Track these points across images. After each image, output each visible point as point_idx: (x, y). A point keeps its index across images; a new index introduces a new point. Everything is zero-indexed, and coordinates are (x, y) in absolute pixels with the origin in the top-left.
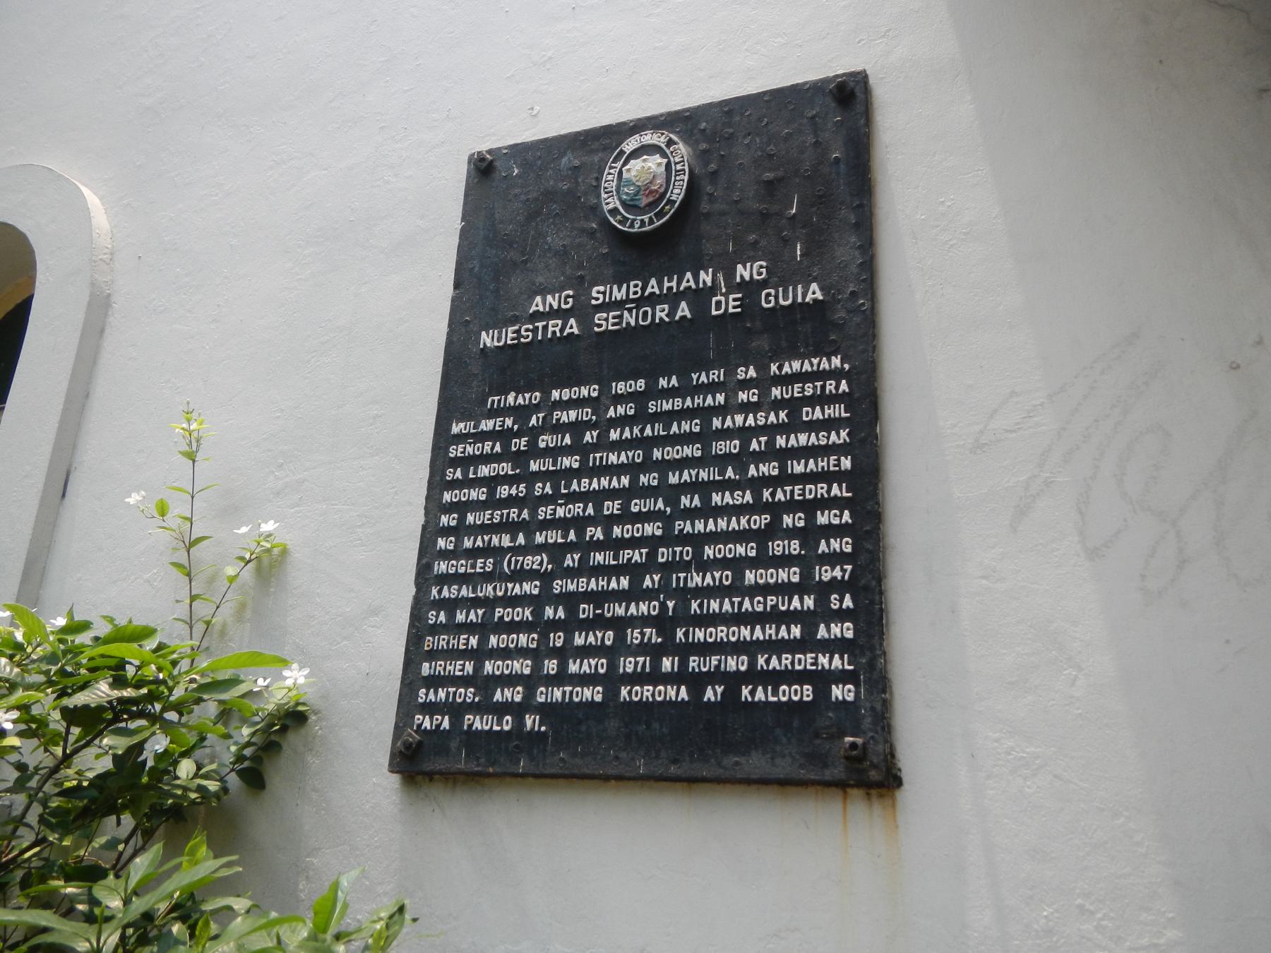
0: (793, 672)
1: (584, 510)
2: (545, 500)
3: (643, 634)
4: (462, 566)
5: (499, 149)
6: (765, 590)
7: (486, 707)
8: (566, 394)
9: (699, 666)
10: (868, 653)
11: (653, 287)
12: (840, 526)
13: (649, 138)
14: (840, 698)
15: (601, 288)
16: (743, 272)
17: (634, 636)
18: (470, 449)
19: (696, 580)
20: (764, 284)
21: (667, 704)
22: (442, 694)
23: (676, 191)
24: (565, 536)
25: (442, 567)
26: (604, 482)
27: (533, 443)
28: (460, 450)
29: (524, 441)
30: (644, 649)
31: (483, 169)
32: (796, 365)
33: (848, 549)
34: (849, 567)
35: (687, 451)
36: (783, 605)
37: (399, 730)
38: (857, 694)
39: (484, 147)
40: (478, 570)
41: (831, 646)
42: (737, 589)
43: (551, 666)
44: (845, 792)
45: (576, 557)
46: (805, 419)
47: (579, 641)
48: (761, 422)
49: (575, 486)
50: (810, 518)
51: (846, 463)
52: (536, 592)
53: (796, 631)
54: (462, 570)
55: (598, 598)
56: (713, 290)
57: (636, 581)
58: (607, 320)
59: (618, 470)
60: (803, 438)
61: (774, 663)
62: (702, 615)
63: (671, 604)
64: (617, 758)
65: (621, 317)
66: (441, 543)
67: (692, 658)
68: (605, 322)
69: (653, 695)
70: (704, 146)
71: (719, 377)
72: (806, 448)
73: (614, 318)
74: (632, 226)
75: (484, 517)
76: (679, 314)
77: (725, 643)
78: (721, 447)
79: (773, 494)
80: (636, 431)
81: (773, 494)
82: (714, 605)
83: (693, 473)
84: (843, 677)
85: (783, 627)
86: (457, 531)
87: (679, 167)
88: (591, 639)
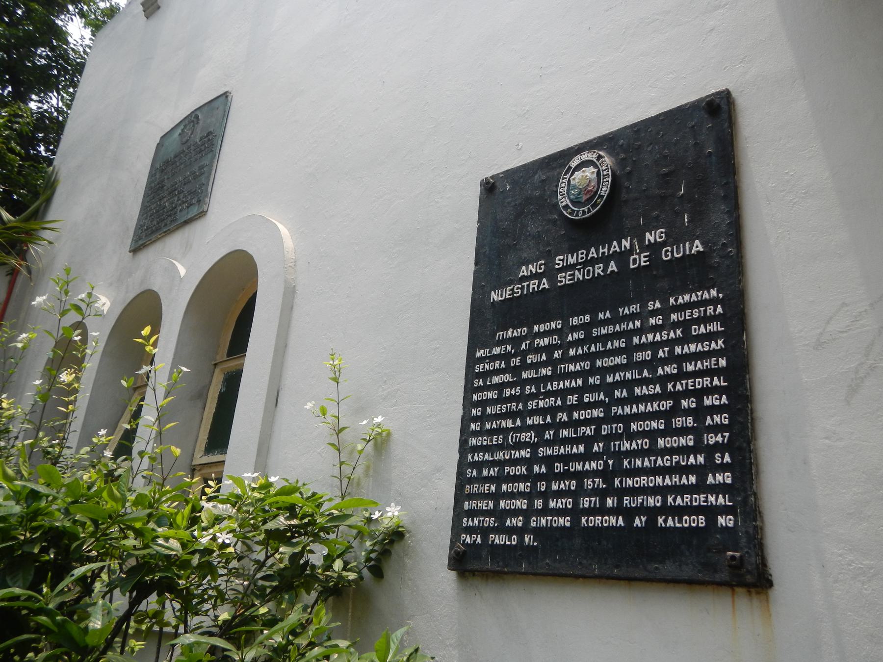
0: (692, 506)
1: (555, 402)
2: (532, 396)
3: (594, 482)
4: (485, 441)
5: (498, 174)
6: (671, 451)
7: (501, 530)
10: (742, 494)
11: (593, 253)
12: (720, 406)
14: (724, 524)
15: (561, 257)
16: (650, 237)
18: (487, 367)
20: (664, 244)
21: (611, 528)
23: (604, 189)
24: (544, 420)
25: (473, 441)
27: (523, 360)
30: (595, 492)
31: (489, 188)
33: (726, 422)
34: (727, 434)
35: (618, 360)
37: (453, 544)
38: (736, 522)
42: (653, 451)
43: (539, 503)
44: (733, 590)
45: (552, 433)
47: (555, 487)
48: (665, 338)
49: (549, 387)
50: (700, 401)
51: (723, 362)
52: (528, 456)
53: (693, 479)
54: (485, 443)
55: (566, 459)
56: (631, 251)
57: (589, 448)
58: (565, 277)
60: (693, 347)
61: (679, 500)
63: (610, 462)
64: (580, 563)
65: (574, 275)
66: (473, 426)
68: (564, 279)
69: (602, 523)
70: (622, 156)
72: (695, 354)
74: (577, 215)
76: (610, 269)
78: (639, 356)
79: (674, 386)
80: (585, 349)
81: (674, 386)
82: (639, 463)
84: (725, 510)
85: (684, 476)
86: (482, 419)
87: (605, 173)
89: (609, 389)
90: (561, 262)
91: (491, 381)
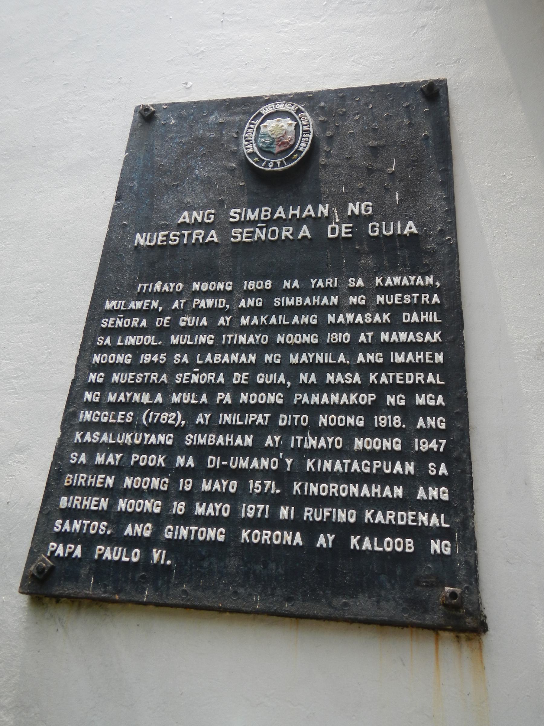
0: (397, 526)
1: (216, 379)
2: (182, 368)
4: (105, 417)
6: (372, 455)
7: (115, 539)
8: (205, 287)
9: (313, 515)
10: (461, 514)
11: (280, 212)
12: (435, 407)
13: (281, 106)
14: (439, 551)
15: (238, 210)
17: (255, 486)
20: (370, 218)
22: (77, 525)
23: (302, 145)
24: (198, 398)
25: (87, 416)
26: (234, 358)
27: (174, 322)
28: (111, 322)
29: (166, 320)
31: (146, 117)
32: (397, 280)
33: (443, 426)
34: (444, 442)
35: (306, 338)
36: (387, 469)
37: (33, 555)
38: (453, 548)
39: (149, 103)
40: (119, 421)
41: (430, 506)
42: (346, 453)
43: (179, 507)
44: (437, 634)
45: (207, 416)
46: (404, 321)
47: (206, 487)
49: (209, 359)
51: (439, 358)
52: (170, 442)
53: (399, 492)
54: (105, 420)
55: (225, 452)
56: (329, 219)
57: (259, 439)
58: (241, 234)
59: (247, 349)
60: (403, 336)
61: (379, 517)
62: (316, 472)
63: (289, 462)
64: (235, 593)
65: (253, 232)
66: (88, 396)
67: (306, 509)
68: (240, 235)
69: (271, 539)
70: (321, 118)
71: (333, 284)
72: (405, 343)
74: (267, 166)
75: (128, 377)
76: (301, 234)
77: (338, 497)
78: (334, 337)
80: (263, 319)
81: (378, 378)
82: (327, 465)
83: (311, 356)
87: (305, 128)
88: (217, 486)
89: (293, 371)
90: (238, 216)
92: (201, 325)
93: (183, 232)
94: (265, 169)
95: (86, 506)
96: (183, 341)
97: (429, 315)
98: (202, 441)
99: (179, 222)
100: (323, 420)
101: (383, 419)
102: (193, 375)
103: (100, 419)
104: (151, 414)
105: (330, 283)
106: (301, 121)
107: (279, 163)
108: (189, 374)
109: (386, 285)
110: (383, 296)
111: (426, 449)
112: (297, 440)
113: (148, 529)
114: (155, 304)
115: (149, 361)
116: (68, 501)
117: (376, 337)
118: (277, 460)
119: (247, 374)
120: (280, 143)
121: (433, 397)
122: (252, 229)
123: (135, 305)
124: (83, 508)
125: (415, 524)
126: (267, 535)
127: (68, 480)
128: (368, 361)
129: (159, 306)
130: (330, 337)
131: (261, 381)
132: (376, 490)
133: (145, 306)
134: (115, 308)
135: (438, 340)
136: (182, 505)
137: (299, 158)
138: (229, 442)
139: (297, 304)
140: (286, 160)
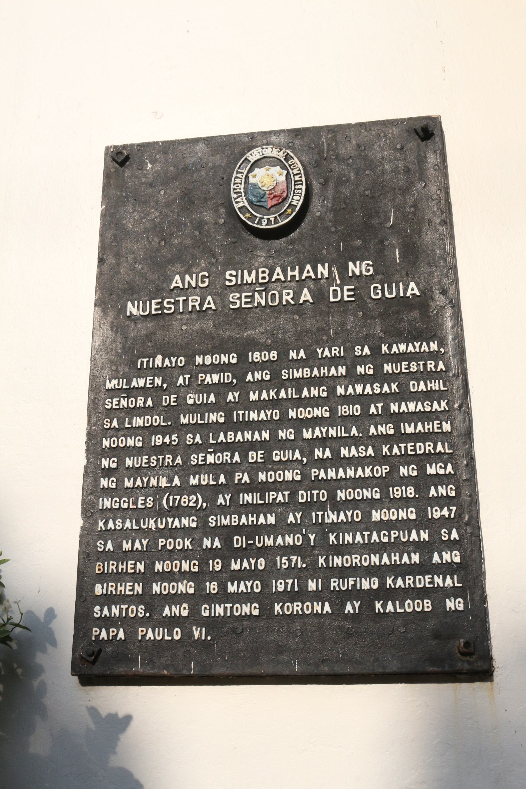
1: (232, 458)
2: (196, 448)
3: (290, 560)
6: (389, 525)
7: (154, 620)
8: (208, 360)
9: (339, 585)
13: (269, 151)
16: (353, 268)
19: (332, 517)
22: (115, 611)
23: (295, 198)
24: (216, 479)
26: (248, 436)
29: (173, 398)
32: (402, 347)
34: (454, 508)
35: (318, 412)
36: (404, 537)
38: (465, 604)
39: (120, 142)
40: (140, 506)
42: (367, 525)
43: (212, 587)
46: (412, 390)
47: (235, 566)
48: (377, 391)
49: (222, 438)
50: (422, 469)
53: (416, 558)
54: (125, 506)
58: (240, 298)
60: (412, 406)
62: (338, 545)
63: (312, 537)
65: (252, 297)
67: (332, 580)
71: (339, 352)
73: (246, 297)
74: (260, 223)
78: (344, 410)
80: (272, 393)
81: (391, 449)
82: (349, 538)
87: (297, 178)
88: (245, 564)
90: (234, 279)
91: (130, 423)
92: (209, 402)
93: (177, 299)
94: (259, 226)
95: (121, 591)
96: (193, 420)
97: (435, 382)
98: (225, 522)
99: (172, 288)
100: (341, 495)
101: (397, 490)
102: (208, 455)
103: (120, 505)
104: (171, 497)
105: (337, 352)
106: (292, 169)
107: (273, 219)
108: (204, 455)
109: (392, 352)
110: (390, 364)
111: (439, 516)
112: (318, 515)
113: (185, 608)
114: (158, 381)
115: (161, 443)
116: (103, 588)
117: (386, 408)
118: (300, 536)
119: (263, 452)
120: (272, 196)
121: (443, 466)
122: (251, 294)
123: (137, 382)
124: (118, 593)
125: (431, 586)
126: (298, 606)
127: (99, 568)
128: (380, 433)
129: (162, 384)
130: (341, 410)
131: (277, 459)
132: (395, 558)
133: (148, 383)
134: (117, 387)
135: (444, 408)
136: (214, 585)
137: (294, 214)
138: (253, 521)
139: (305, 376)
140: (280, 215)
